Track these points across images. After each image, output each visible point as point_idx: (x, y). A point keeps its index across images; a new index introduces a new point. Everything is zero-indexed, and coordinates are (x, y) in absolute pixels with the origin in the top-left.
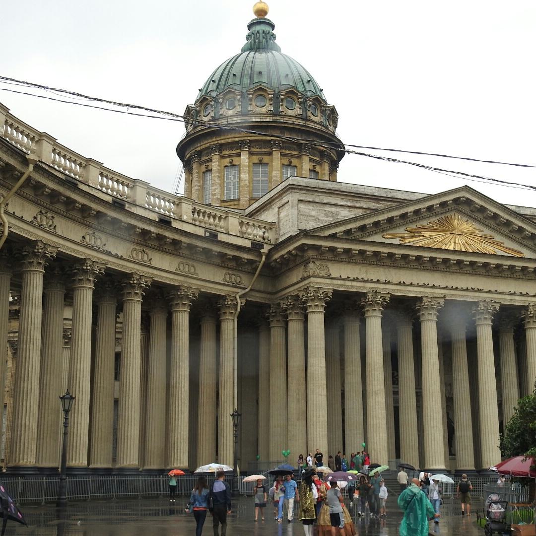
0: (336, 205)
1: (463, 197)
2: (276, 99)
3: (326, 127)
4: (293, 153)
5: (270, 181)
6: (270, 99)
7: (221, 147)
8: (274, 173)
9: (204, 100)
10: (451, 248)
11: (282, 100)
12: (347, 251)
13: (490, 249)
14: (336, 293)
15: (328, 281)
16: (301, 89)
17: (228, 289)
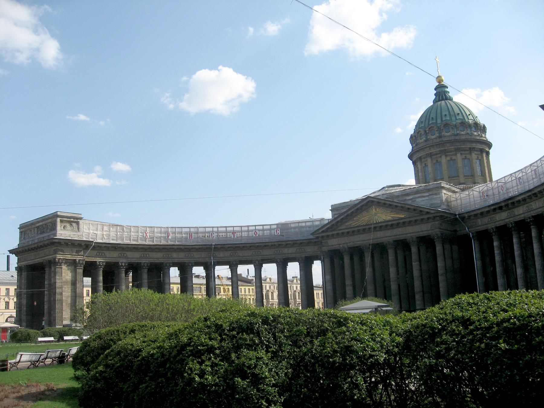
1: (370, 200)
3: (457, 135)
4: (438, 156)
6: (423, 134)
11: (428, 133)
12: (333, 235)
13: (389, 218)
16: (439, 121)
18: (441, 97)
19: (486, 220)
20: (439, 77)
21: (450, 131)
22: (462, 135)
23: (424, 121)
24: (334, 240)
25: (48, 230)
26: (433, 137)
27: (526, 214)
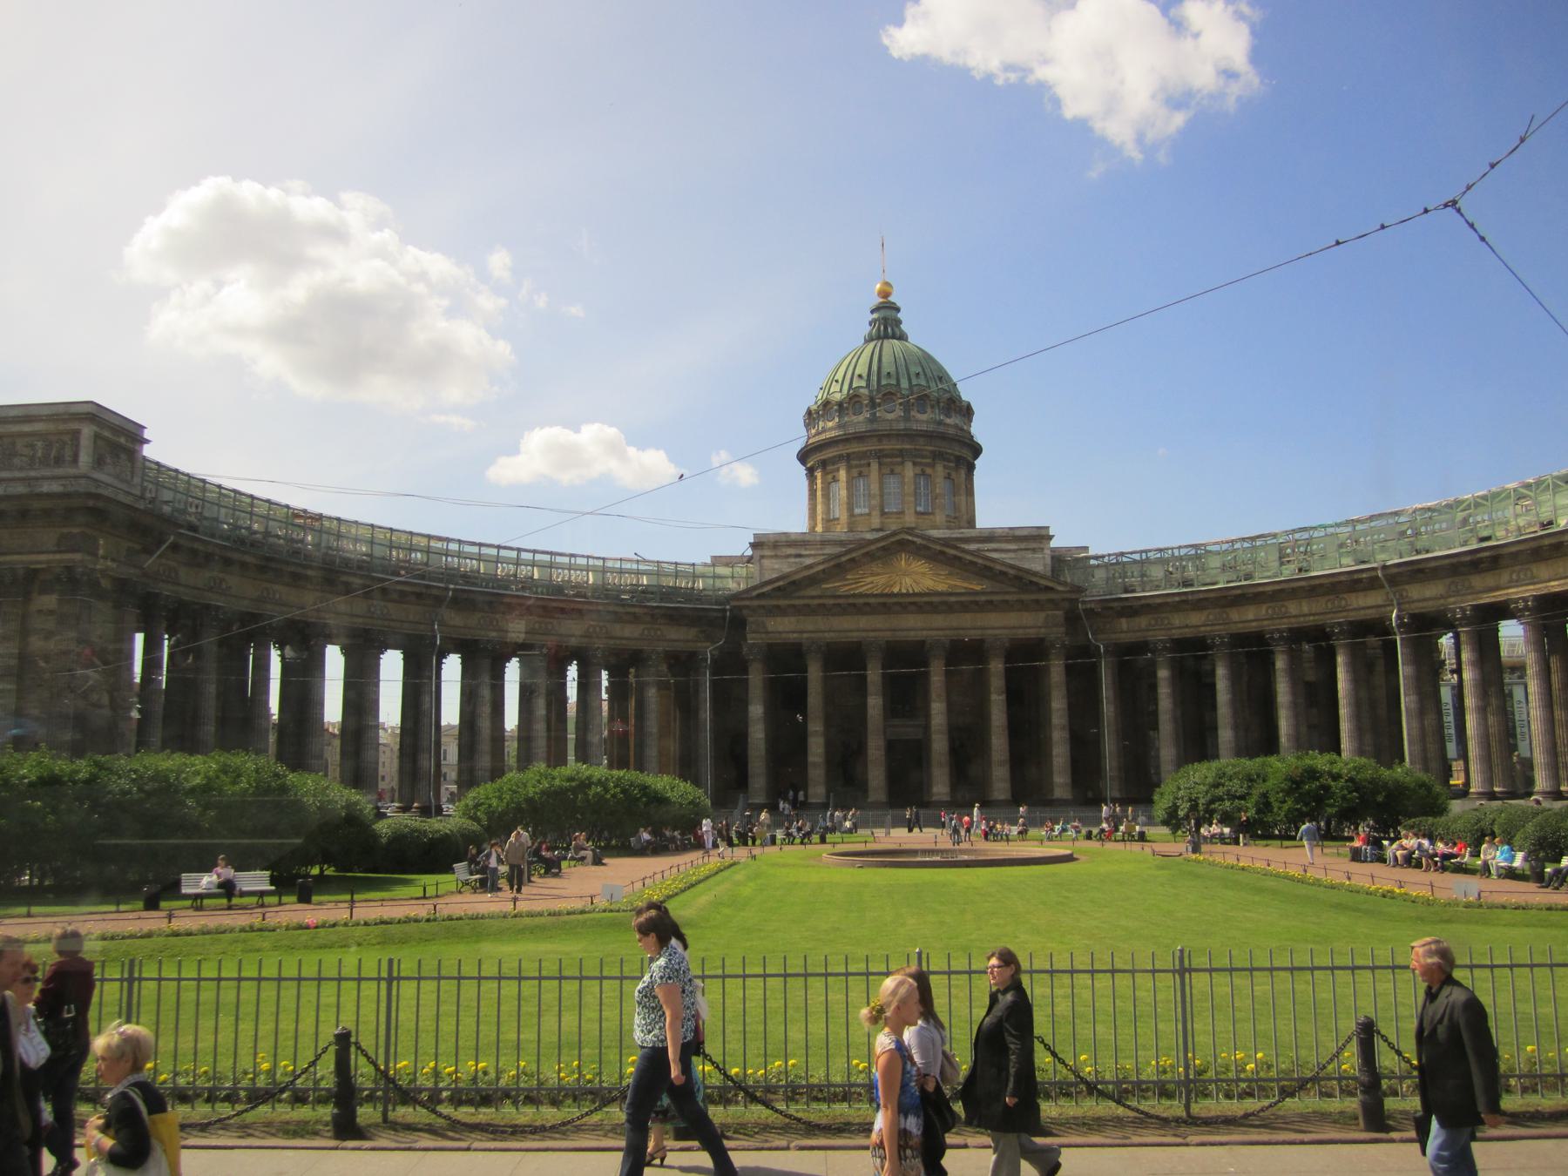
0: (800, 556)
2: (873, 404)
3: (940, 423)
4: (895, 460)
5: (869, 495)
7: (824, 464)
8: (872, 487)
9: (809, 412)
10: (896, 590)
11: (879, 405)
13: (941, 587)
14: (770, 645)
15: (763, 636)
16: (904, 384)
17: (699, 644)
18: (889, 330)
19: (1143, 621)
20: (887, 284)
21: (925, 412)
22: (948, 425)
23: (865, 375)
24: (786, 620)
25: (16, 461)
26: (890, 416)
27: (1266, 623)
